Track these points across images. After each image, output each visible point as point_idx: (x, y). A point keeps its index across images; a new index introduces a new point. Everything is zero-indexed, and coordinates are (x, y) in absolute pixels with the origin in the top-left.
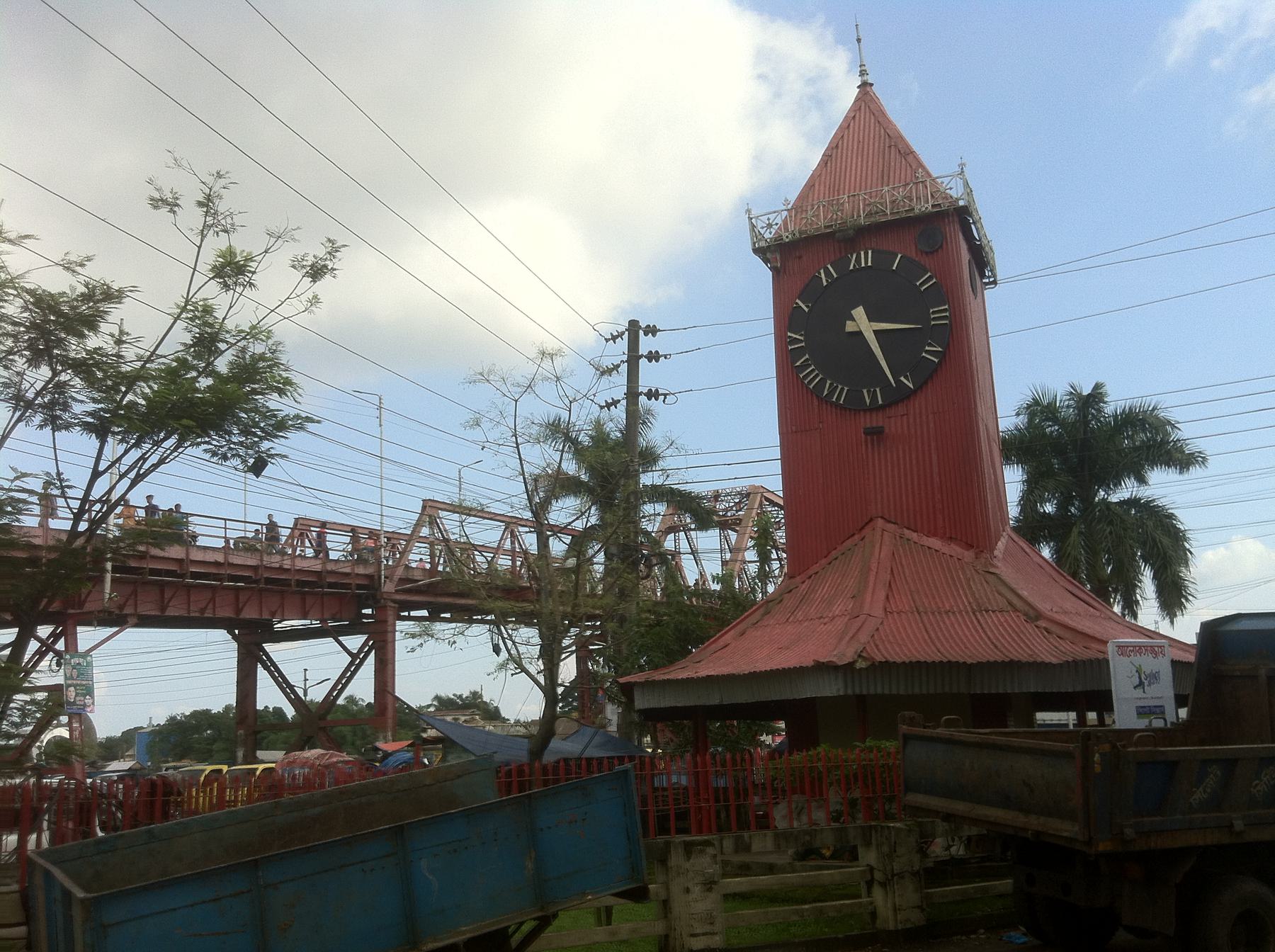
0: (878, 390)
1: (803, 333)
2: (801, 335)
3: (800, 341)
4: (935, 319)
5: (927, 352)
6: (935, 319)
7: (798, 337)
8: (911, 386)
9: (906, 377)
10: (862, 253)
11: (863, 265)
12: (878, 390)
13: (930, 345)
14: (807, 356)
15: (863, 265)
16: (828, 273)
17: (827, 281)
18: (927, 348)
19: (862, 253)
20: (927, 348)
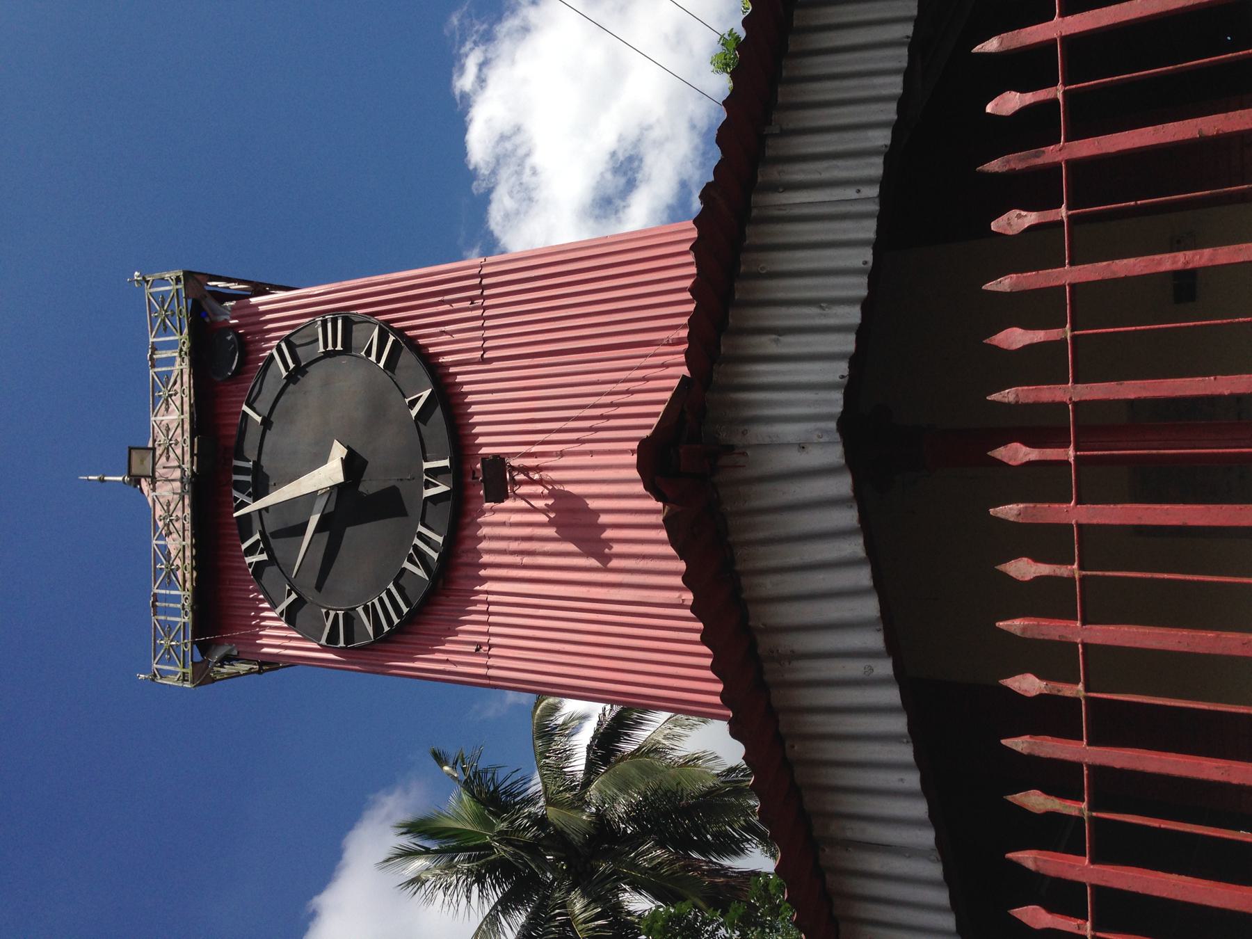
0: (427, 465)
1: (324, 611)
2: (327, 614)
3: (336, 616)
4: (335, 344)
5: (379, 358)
6: (335, 344)
7: (328, 624)
8: (426, 393)
9: (413, 404)
10: (236, 477)
11: (248, 478)
12: (427, 465)
13: (369, 353)
14: (360, 610)
15: (248, 478)
16: (251, 551)
17: (261, 552)
18: (373, 358)
19: (236, 477)
20: (373, 358)
